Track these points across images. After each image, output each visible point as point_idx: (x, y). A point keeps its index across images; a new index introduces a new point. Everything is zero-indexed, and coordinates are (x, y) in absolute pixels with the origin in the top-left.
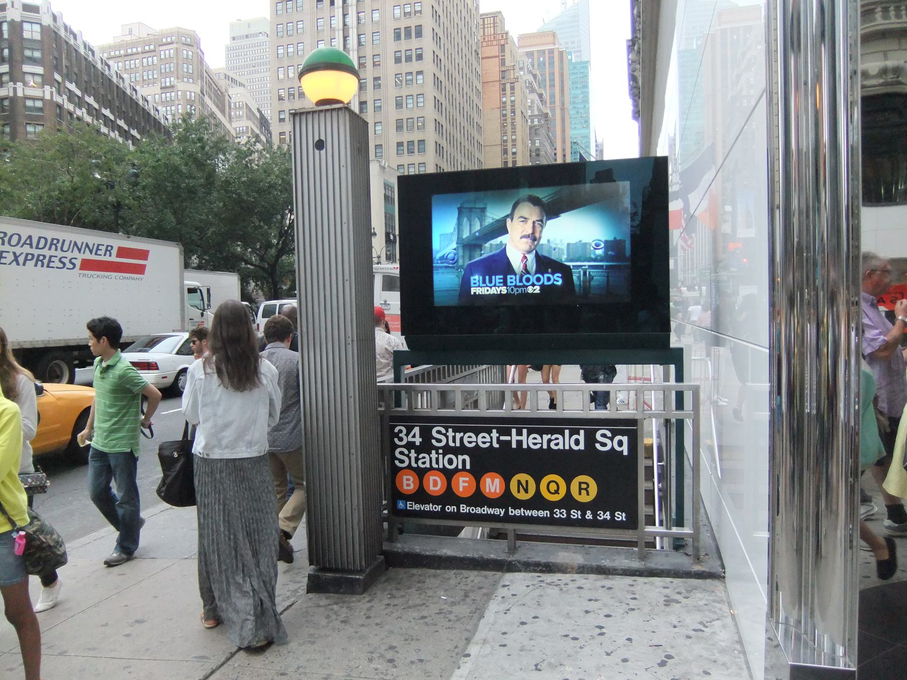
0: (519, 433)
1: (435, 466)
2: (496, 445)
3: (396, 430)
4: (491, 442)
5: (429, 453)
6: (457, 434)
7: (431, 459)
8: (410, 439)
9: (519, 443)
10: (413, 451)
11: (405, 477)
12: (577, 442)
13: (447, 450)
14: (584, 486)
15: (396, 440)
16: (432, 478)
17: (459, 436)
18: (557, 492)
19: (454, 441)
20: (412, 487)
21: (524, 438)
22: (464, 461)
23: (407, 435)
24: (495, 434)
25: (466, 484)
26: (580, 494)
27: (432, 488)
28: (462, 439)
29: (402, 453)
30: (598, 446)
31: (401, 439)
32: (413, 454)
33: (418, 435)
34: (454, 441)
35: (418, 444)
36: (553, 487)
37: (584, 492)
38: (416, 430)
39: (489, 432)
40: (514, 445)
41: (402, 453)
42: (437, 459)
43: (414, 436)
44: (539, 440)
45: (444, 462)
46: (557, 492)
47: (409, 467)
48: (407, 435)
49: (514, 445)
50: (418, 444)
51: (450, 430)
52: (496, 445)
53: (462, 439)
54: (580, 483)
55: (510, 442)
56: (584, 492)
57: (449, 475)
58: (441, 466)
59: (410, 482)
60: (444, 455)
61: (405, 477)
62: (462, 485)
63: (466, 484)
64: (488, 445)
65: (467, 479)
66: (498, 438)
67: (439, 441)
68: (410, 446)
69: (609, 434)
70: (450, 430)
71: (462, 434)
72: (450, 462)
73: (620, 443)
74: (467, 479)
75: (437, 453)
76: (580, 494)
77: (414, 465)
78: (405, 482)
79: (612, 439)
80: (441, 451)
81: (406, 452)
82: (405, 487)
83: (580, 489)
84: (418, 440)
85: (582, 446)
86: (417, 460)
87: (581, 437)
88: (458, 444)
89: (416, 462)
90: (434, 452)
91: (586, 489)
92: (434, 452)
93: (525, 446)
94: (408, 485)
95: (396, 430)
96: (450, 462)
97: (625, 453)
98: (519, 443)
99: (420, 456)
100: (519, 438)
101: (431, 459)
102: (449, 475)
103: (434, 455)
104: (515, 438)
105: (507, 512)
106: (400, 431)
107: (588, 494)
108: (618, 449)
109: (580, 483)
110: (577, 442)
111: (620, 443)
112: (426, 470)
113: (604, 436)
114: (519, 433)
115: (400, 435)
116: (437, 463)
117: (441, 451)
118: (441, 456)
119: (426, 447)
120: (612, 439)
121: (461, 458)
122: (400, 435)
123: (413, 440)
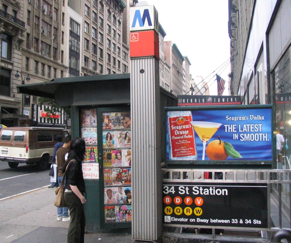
3: (164, 188)
8: (170, 191)
15: (164, 192)
23: (169, 190)
31: (166, 191)
33: (173, 190)
35: (173, 193)
38: (173, 188)
43: (172, 190)
48: (169, 190)
50: (173, 193)
84: (173, 192)
95: (164, 188)
105: (209, 221)
106: (166, 188)
115: (166, 190)
122: (166, 190)
123: (171, 192)
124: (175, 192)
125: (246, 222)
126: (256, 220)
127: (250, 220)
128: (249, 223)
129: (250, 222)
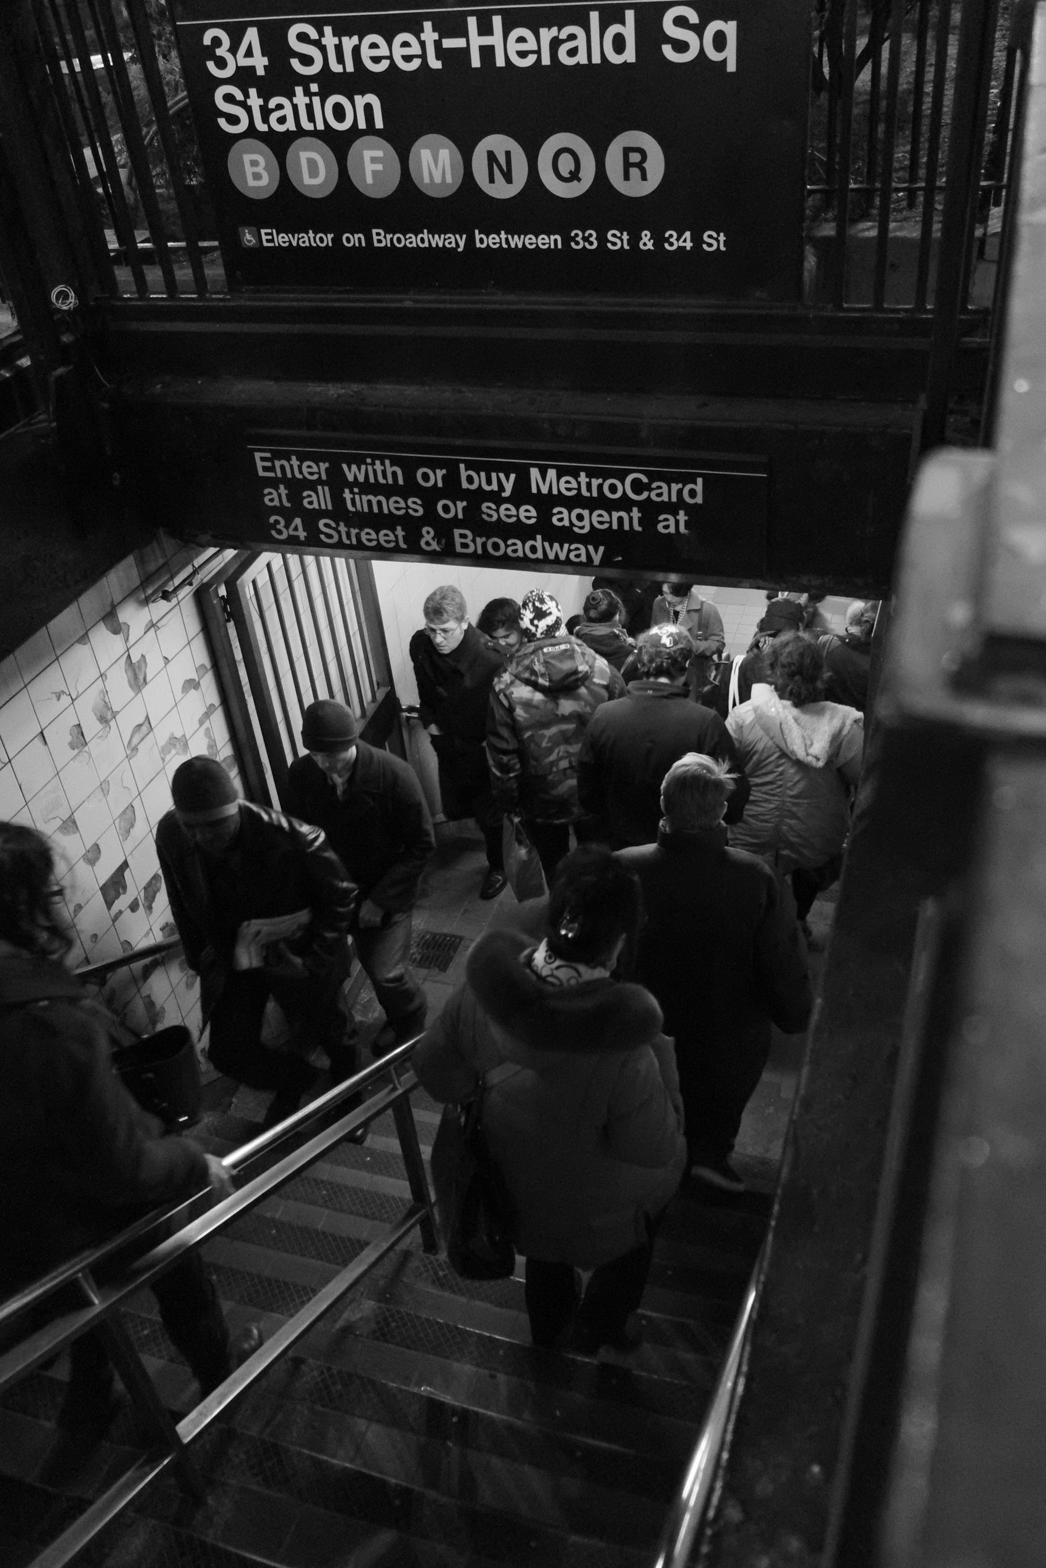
0: (485, 29)
1: (307, 126)
2: (435, 64)
4: (423, 56)
5: (290, 95)
6: (345, 40)
7: (295, 108)
9: (487, 52)
10: (253, 92)
11: (247, 158)
12: (619, 43)
13: (329, 83)
14: (635, 157)
16: (304, 156)
18: (575, 176)
20: (265, 181)
21: (495, 40)
24: (429, 35)
25: (379, 167)
26: (627, 177)
27: (307, 180)
29: (229, 98)
32: (255, 101)
36: (566, 164)
37: (635, 172)
40: (476, 62)
41: (229, 98)
42: (310, 107)
45: (324, 115)
46: (575, 176)
47: (251, 132)
49: (476, 62)
51: (328, 30)
52: (435, 64)
53: (356, 51)
54: (627, 151)
56: (635, 172)
57: (339, 144)
58: (320, 126)
59: (260, 169)
61: (247, 158)
62: (369, 168)
63: (379, 167)
65: (379, 154)
66: (438, 44)
67: (307, 60)
68: (244, 77)
69: (693, 17)
70: (328, 30)
71: (355, 40)
72: (339, 112)
73: (720, 42)
74: (379, 154)
75: (307, 93)
76: (627, 177)
77: (262, 127)
78: (249, 170)
79: (699, 30)
80: (314, 88)
82: (252, 183)
83: (627, 165)
85: (630, 55)
86: (266, 113)
87: (629, 30)
89: (265, 120)
90: (299, 90)
91: (640, 165)
92: (299, 90)
93: (500, 62)
94: (257, 176)
96: (339, 112)
97: (731, 67)
98: (487, 52)
99: (272, 103)
100: (486, 41)
101: (295, 108)
102: (339, 144)
103: (300, 99)
107: (644, 177)
109: (627, 151)
111: (720, 42)
112: (289, 138)
114: (485, 29)
116: (311, 118)
117: (314, 88)
118: (316, 100)
119: (279, 80)
120: (699, 30)
125: (671, 244)
126: (715, 235)
127: (687, 235)
128: (681, 249)
129: (689, 245)
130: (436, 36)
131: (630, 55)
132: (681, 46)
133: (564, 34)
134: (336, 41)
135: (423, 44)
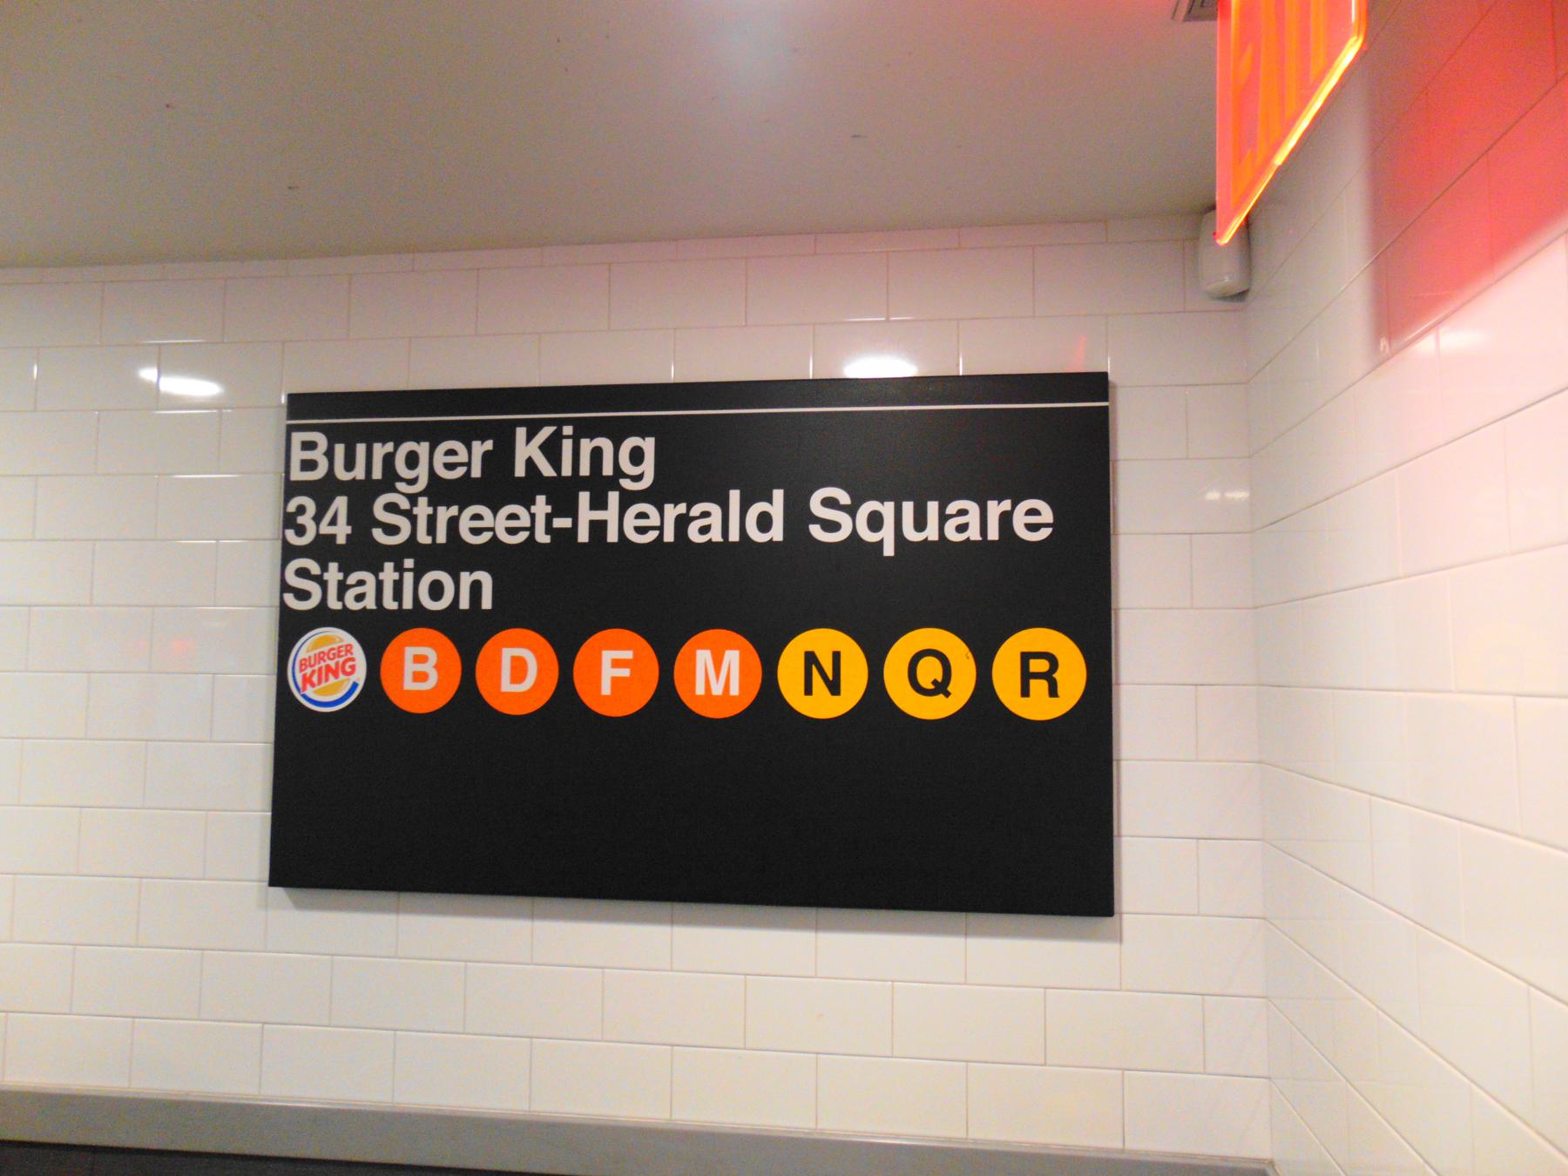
2: (542, 537)
4: (532, 529)
5: (376, 569)
9: (598, 528)
17: (444, 514)
19: (432, 530)
21: (610, 515)
22: (476, 587)
23: (318, 519)
24: (541, 506)
28: (453, 523)
30: (816, 531)
34: (432, 530)
35: (341, 540)
39: (528, 503)
40: (583, 536)
43: (333, 522)
44: (654, 520)
49: (583, 536)
50: (341, 540)
53: (453, 523)
55: (574, 529)
60: (418, 575)
64: (522, 537)
66: (549, 518)
69: (844, 498)
71: (454, 510)
79: (852, 511)
81: (314, 568)
84: (342, 532)
85: (777, 533)
86: (343, 588)
88: (442, 538)
98: (598, 528)
100: (598, 515)
104: (586, 514)
108: (867, 536)
110: (765, 522)
113: (830, 503)
114: (599, 503)
120: (852, 511)
121: (466, 579)
124: (349, 530)
130: (549, 509)
131: (777, 533)
132: (832, 526)
133: (696, 510)
134: (430, 511)
135: (533, 516)
